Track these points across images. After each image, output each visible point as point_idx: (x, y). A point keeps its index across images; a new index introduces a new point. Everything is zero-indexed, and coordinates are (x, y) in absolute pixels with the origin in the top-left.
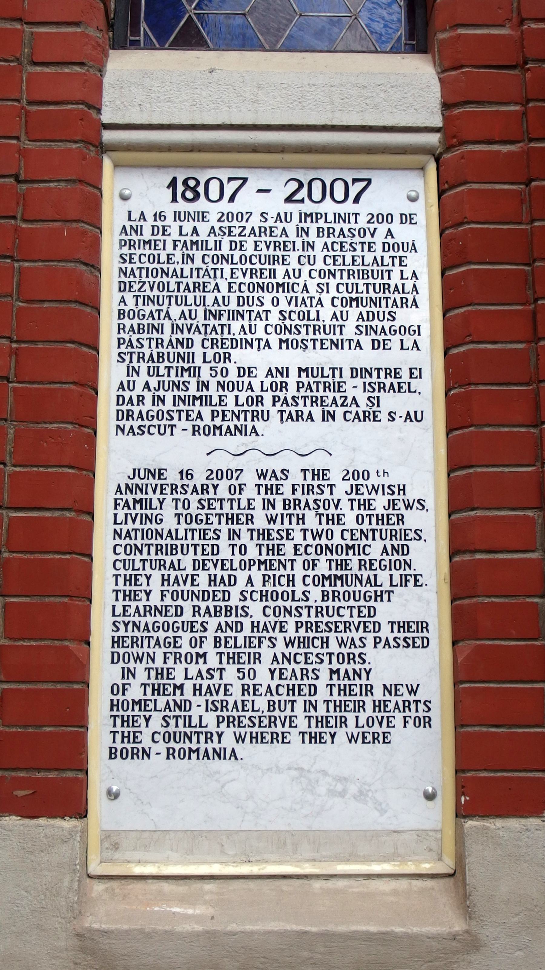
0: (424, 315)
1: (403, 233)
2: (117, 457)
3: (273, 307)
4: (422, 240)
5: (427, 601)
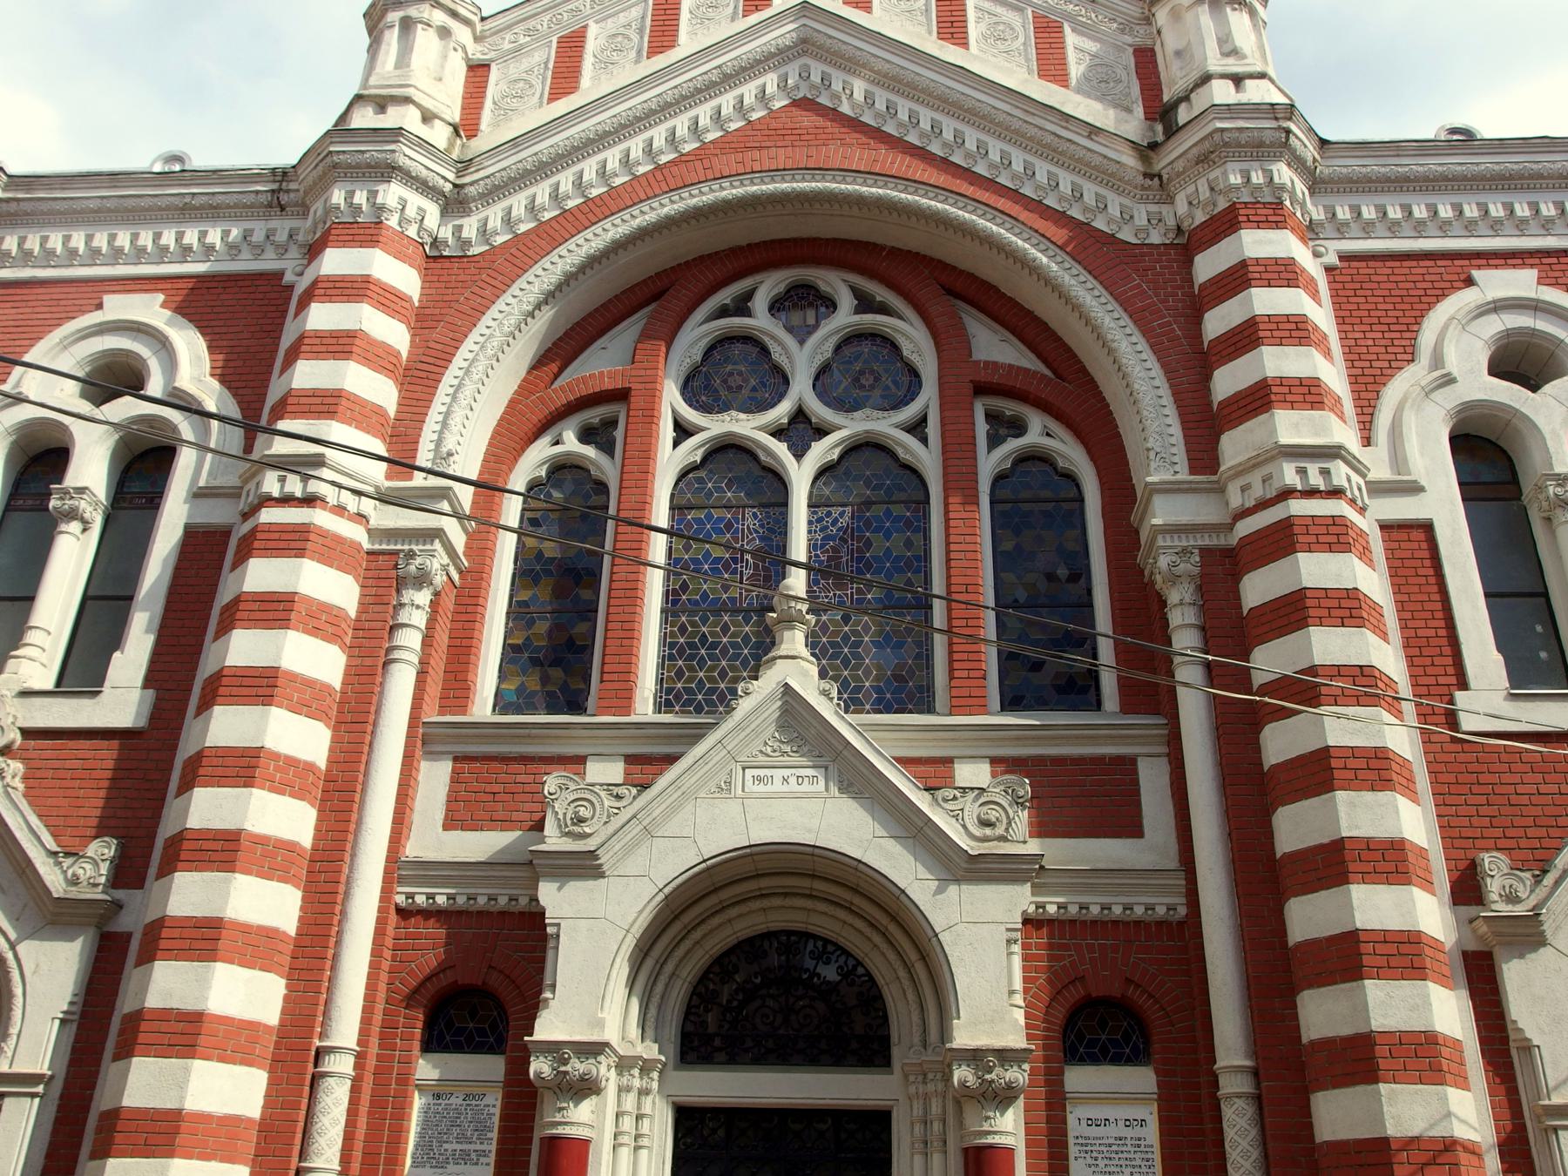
0: (494, 1135)
1: (492, 1110)
3: (456, 1130)
4: (497, 1111)
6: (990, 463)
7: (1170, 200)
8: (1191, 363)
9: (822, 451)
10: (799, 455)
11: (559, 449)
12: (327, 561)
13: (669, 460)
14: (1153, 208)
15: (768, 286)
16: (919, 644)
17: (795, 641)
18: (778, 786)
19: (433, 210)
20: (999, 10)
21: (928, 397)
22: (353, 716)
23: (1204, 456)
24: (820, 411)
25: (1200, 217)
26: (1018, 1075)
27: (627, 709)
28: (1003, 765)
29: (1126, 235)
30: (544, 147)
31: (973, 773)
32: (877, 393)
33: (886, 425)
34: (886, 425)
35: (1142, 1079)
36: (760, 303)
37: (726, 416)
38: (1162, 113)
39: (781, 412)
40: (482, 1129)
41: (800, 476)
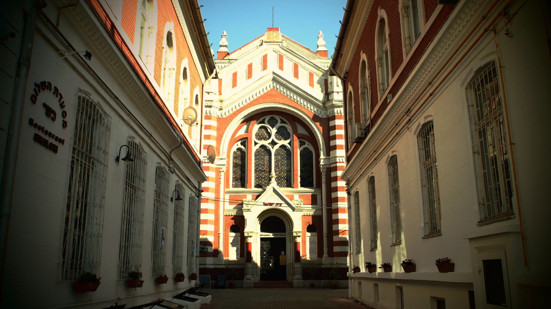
9: (277, 147)
10: (273, 148)
11: (238, 147)
13: (254, 149)
15: (267, 118)
17: (273, 180)
22: (217, 191)
23: (328, 154)
24: (276, 141)
26: (300, 234)
27: (251, 188)
28: (300, 197)
29: (320, 116)
31: (296, 197)
36: (266, 121)
40: (238, 241)
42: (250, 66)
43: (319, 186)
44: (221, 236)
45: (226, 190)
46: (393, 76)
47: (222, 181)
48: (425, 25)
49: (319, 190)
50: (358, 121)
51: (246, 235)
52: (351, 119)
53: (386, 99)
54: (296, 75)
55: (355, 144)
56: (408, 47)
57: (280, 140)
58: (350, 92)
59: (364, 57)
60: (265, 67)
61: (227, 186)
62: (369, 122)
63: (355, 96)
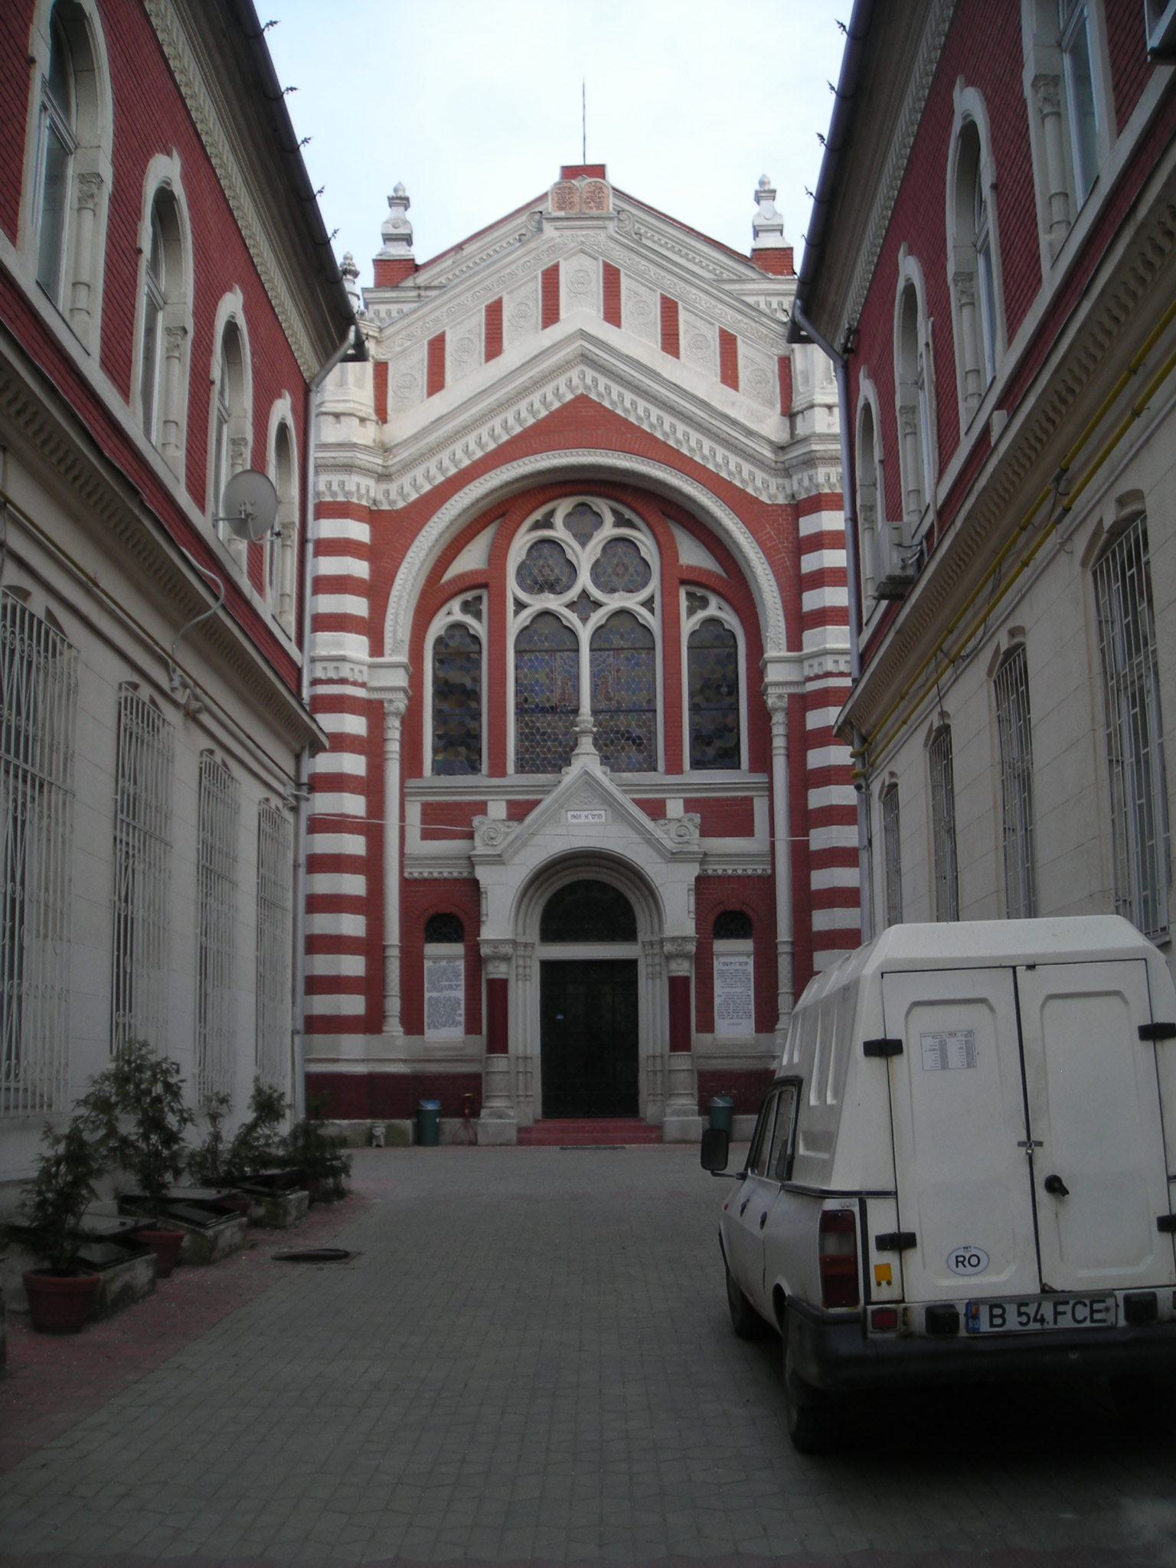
0: (463, 977)
2: (427, 995)
5: (462, 1011)
6: (688, 625)
7: (790, 477)
8: (796, 584)
9: (597, 618)
10: (584, 620)
12: (353, 712)
13: (515, 624)
14: (780, 481)
15: (564, 507)
16: (650, 732)
17: (586, 744)
18: (583, 820)
19: (371, 483)
20: (699, 323)
21: (654, 586)
23: (795, 644)
24: (596, 594)
25: (804, 496)
28: (690, 805)
29: (764, 498)
30: (432, 438)
31: (675, 808)
32: (627, 578)
33: (631, 602)
34: (631, 602)
35: (747, 945)
37: (543, 596)
38: (790, 414)
39: (573, 594)
40: (457, 975)
41: (585, 634)
42: (494, 312)
43: (762, 762)
44: (394, 955)
45: (412, 783)
46: (1010, 340)
47: (394, 747)
48: (1111, 148)
49: (761, 778)
50: (894, 512)
51: (485, 950)
52: (870, 508)
53: (987, 430)
54: (670, 343)
55: (884, 603)
56: (1060, 232)
57: (613, 590)
58: (867, 407)
59: (910, 268)
60: (551, 315)
61: (411, 765)
62: (931, 517)
63: (882, 422)
